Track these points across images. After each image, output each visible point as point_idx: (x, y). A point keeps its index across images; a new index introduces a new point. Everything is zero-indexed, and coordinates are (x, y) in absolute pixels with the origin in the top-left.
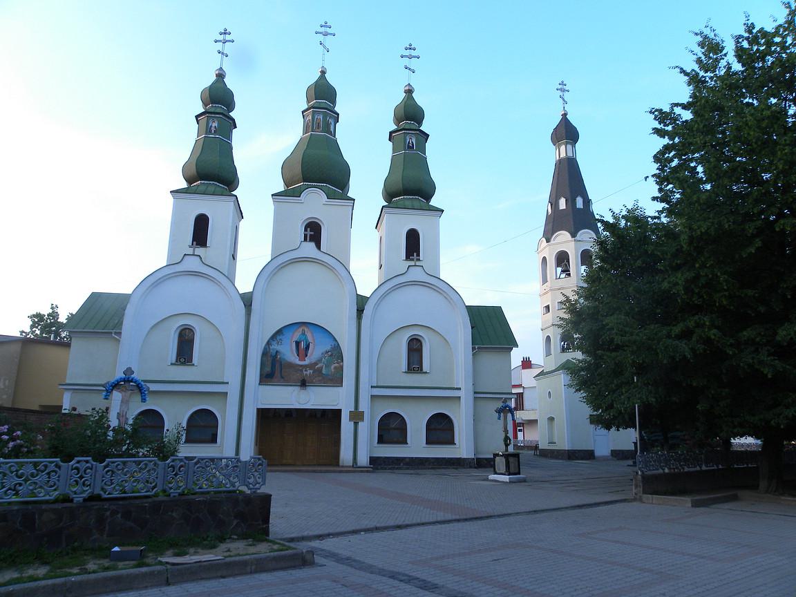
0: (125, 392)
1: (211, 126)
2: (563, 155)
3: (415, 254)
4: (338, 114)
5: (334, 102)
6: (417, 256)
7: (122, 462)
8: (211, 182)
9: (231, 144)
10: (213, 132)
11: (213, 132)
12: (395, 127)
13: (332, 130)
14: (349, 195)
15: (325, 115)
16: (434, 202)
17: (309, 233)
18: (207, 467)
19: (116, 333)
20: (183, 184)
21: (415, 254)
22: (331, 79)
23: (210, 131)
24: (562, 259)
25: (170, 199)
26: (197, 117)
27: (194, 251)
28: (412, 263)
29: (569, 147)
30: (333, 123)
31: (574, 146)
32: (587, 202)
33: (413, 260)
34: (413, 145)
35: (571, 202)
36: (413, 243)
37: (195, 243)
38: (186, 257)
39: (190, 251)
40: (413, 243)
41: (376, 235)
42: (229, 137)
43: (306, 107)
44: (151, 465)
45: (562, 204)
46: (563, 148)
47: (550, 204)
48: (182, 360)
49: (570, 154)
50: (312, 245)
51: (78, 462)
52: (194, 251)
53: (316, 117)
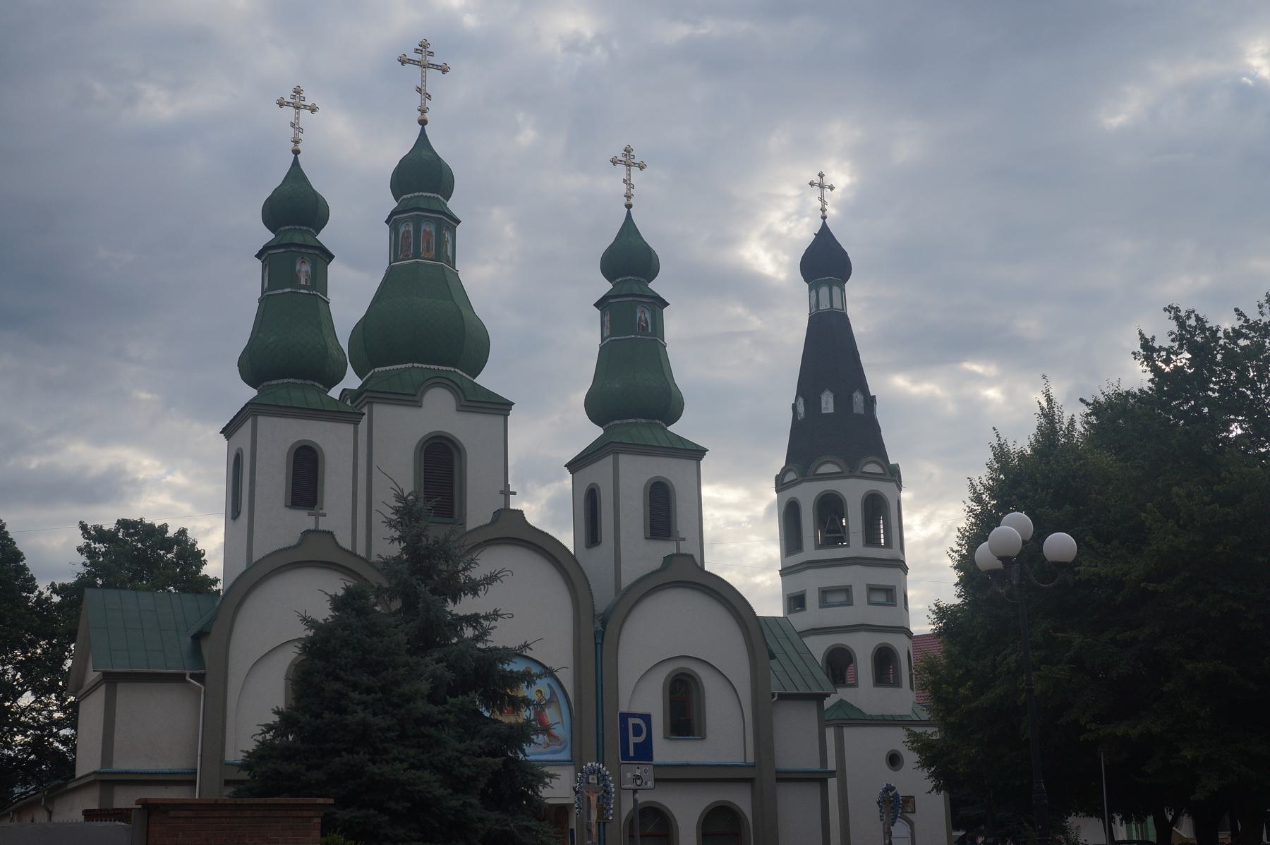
2: (825, 306)
8: (309, 382)
11: (303, 282)
13: (449, 254)
15: (439, 223)
19: (192, 676)
22: (441, 146)
23: (297, 279)
24: (830, 508)
27: (317, 522)
29: (836, 290)
30: (450, 240)
31: (843, 290)
32: (870, 402)
35: (843, 401)
45: (828, 403)
46: (824, 291)
47: (801, 400)
49: (837, 305)
52: (317, 522)
53: (423, 227)
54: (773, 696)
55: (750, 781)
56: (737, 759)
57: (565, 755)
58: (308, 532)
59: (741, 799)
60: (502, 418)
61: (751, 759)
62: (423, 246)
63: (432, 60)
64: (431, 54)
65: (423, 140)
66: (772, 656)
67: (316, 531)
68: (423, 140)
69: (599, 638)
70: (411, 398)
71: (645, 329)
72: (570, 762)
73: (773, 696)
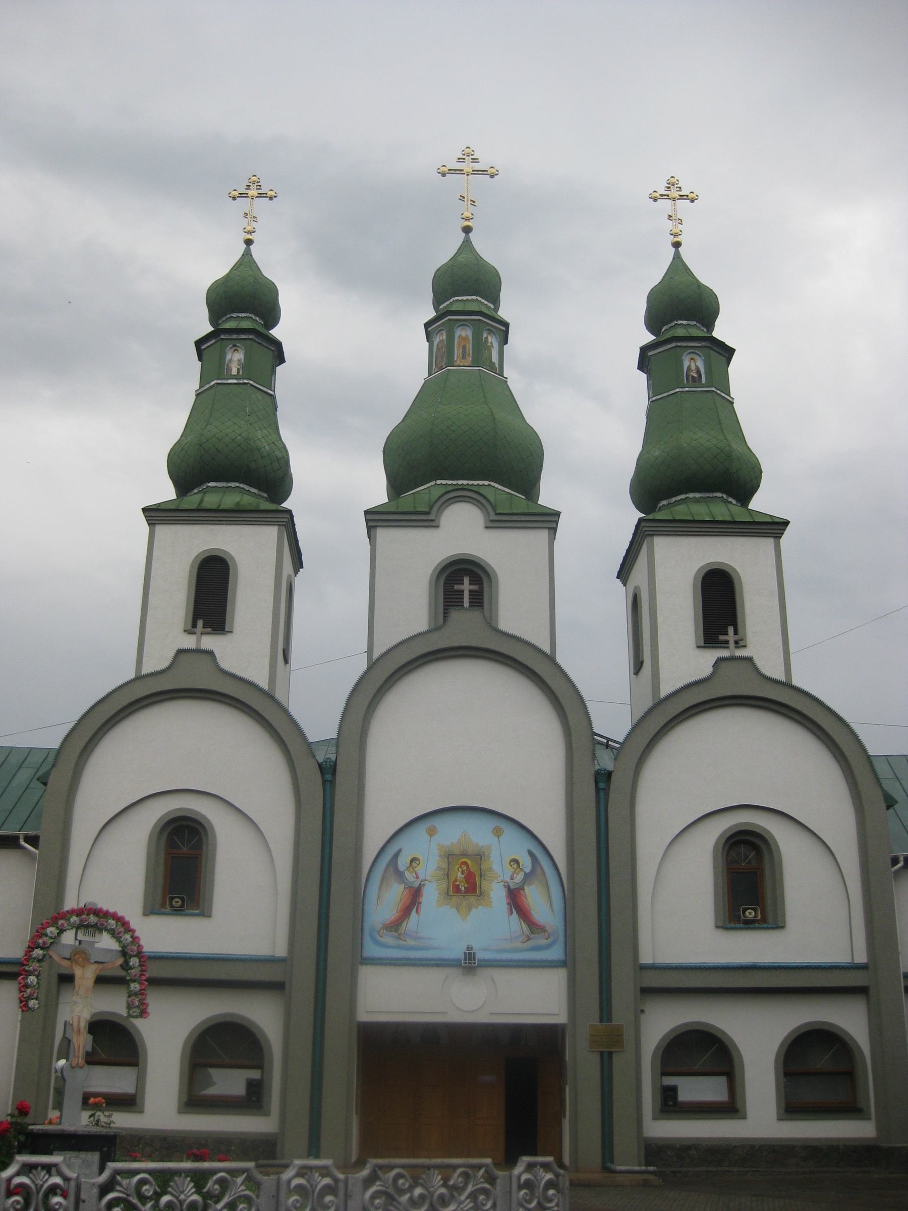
0: (83, 967)
1: (230, 361)
3: (731, 630)
4: (506, 325)
5: (496, 301)
6: (736, 633)
7: (150, 1172)
8: (233, 484)
9: (273, 397)
10: (234, 372)
11: (234, 372)
12: (650, 338)
13: (495, 359)
14: (547, 498)
16: (762, 502)
17: (466, 586)
18: (401, 1192)
20: (166, 492)
21: (731, 630)
23: (229, 369)
25: (143, 526)
26: (199, 343)
27: (199, 641)
28: (725, 653)
30: (496, 345)
33: (725, 644)
34: (700, 375)
36: (719, 602)
37: (200, 623)
38: (184, 657)
39: (189, 642)
40: (719, 602)
41: (619, 595)
42: (269, 379)
43: (432, 314)
44: (239, 1187)
48: (177, 902)
50: (474, 616)
51: (28, 1169)
52: (199, 641)
54: (895, 861)
55: (861, 991)
56: (841, 957)
57: (556, 953)
58: (180, 652)
59: (850, 1020)
60: (544, 534)
61: (861, 957)
62: (457, 351)
63: (477, 166)
64: (475, 160)
65: (467, 245)
66: (890, 802)
67: (198, 651)
68: (467, 245)
69: (603, 778)
70: (424, 518)
71: (696, 380)
72: (563, 964)
73: (895, 861)
